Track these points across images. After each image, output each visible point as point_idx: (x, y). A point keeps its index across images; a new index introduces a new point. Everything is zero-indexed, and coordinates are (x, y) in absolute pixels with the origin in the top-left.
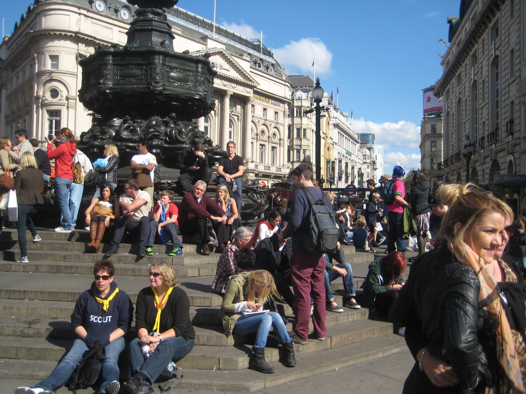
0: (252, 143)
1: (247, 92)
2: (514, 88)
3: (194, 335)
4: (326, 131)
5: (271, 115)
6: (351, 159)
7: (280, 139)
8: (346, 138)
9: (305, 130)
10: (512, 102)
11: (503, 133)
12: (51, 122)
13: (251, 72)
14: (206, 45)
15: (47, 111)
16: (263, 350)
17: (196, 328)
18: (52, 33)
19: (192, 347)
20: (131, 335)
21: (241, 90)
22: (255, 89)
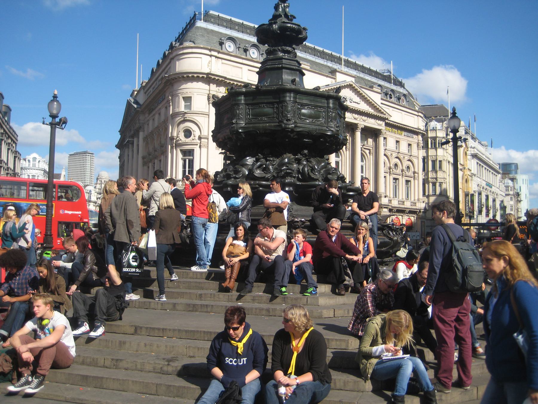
0: (385, 177)
1: (379, 125)
3: (331, 379)
4: (464, 162)
5: (403, 148)
7: (414, 173)
8: (485, 168)
9: (440, 161)
12: (185, 161)
13: (382, 103)
14: (334, 79)
15: (181, 150)
16: (403, 397)
17: (332, 372)
18: (185, 76)
19: (328, 392)
20: (266, 377)
21: (372, 123)
22: (387, 121)
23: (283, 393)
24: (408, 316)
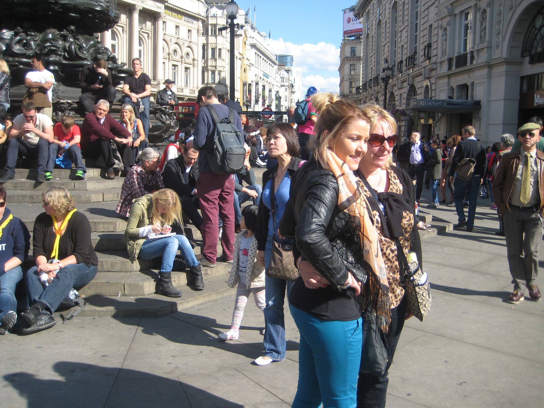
0: (164, 63)
1: (158, 7)
2: (433, 11)
3: (97, 261)
7: (194, 60)
9: (220, 49)
10: (431, 26)
11: (420, 57)
16: (169, 274)
17: (98, 254)
19: (95, 274)
20: (28, 264)
22: (166, 4)
23: (46, 280)
24: (174, 194)
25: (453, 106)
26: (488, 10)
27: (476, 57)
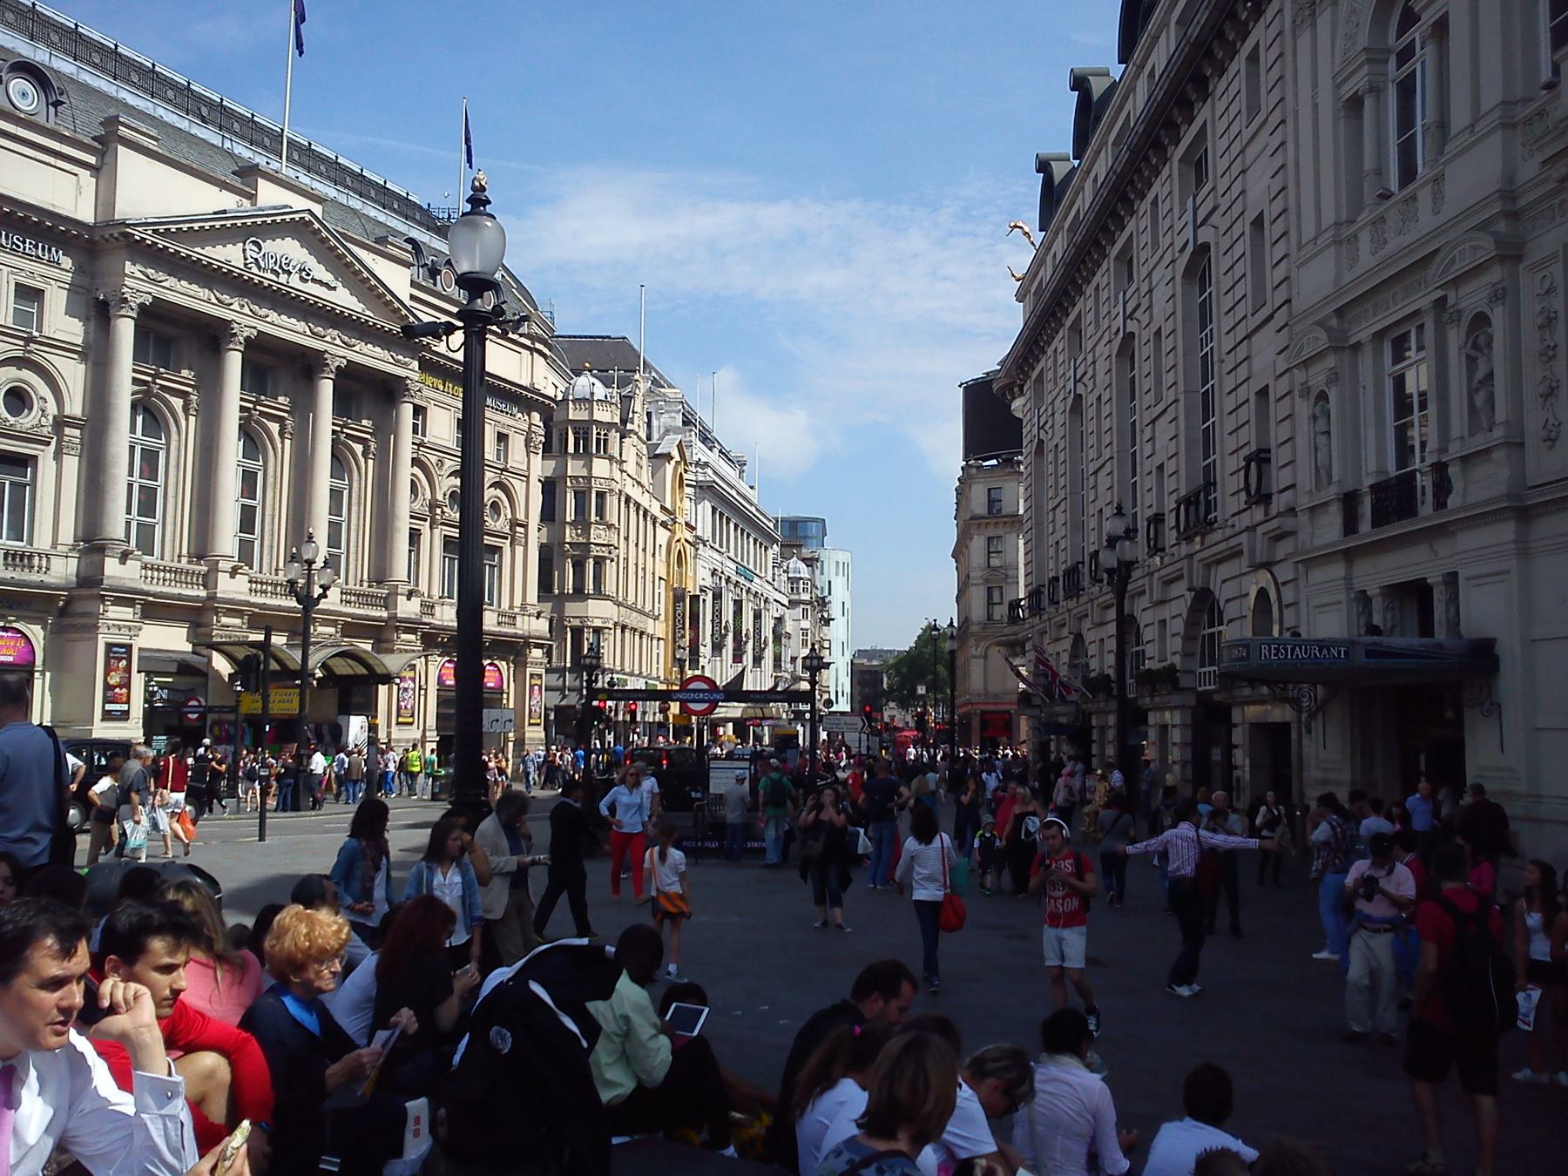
2: (1266, 347)
4: (674, 502)
6: (753, 590)
7: (514, 523)
10: (1263, 393)
11: (1229, 497)
13: (413, 297)
25: (1388, 662)
26: (1498, 316)
27: (1457, 485)
